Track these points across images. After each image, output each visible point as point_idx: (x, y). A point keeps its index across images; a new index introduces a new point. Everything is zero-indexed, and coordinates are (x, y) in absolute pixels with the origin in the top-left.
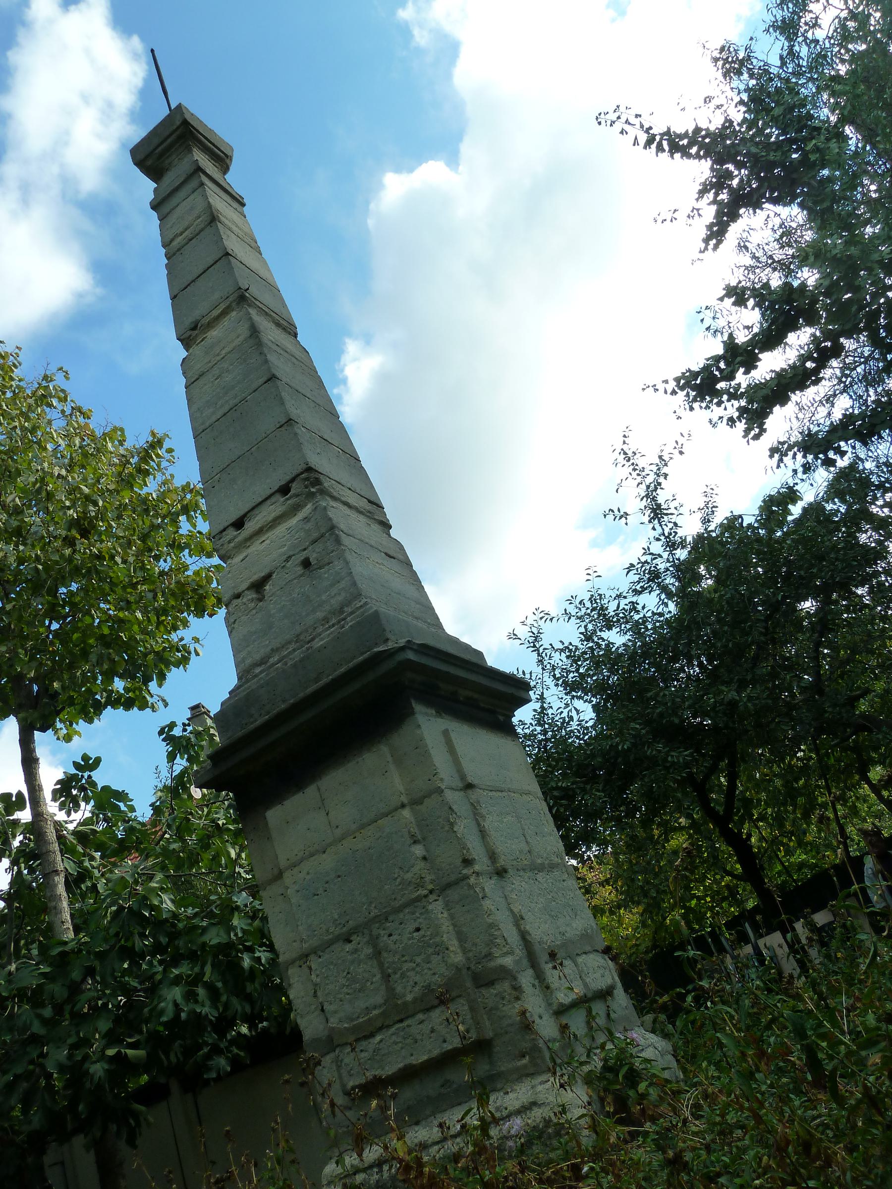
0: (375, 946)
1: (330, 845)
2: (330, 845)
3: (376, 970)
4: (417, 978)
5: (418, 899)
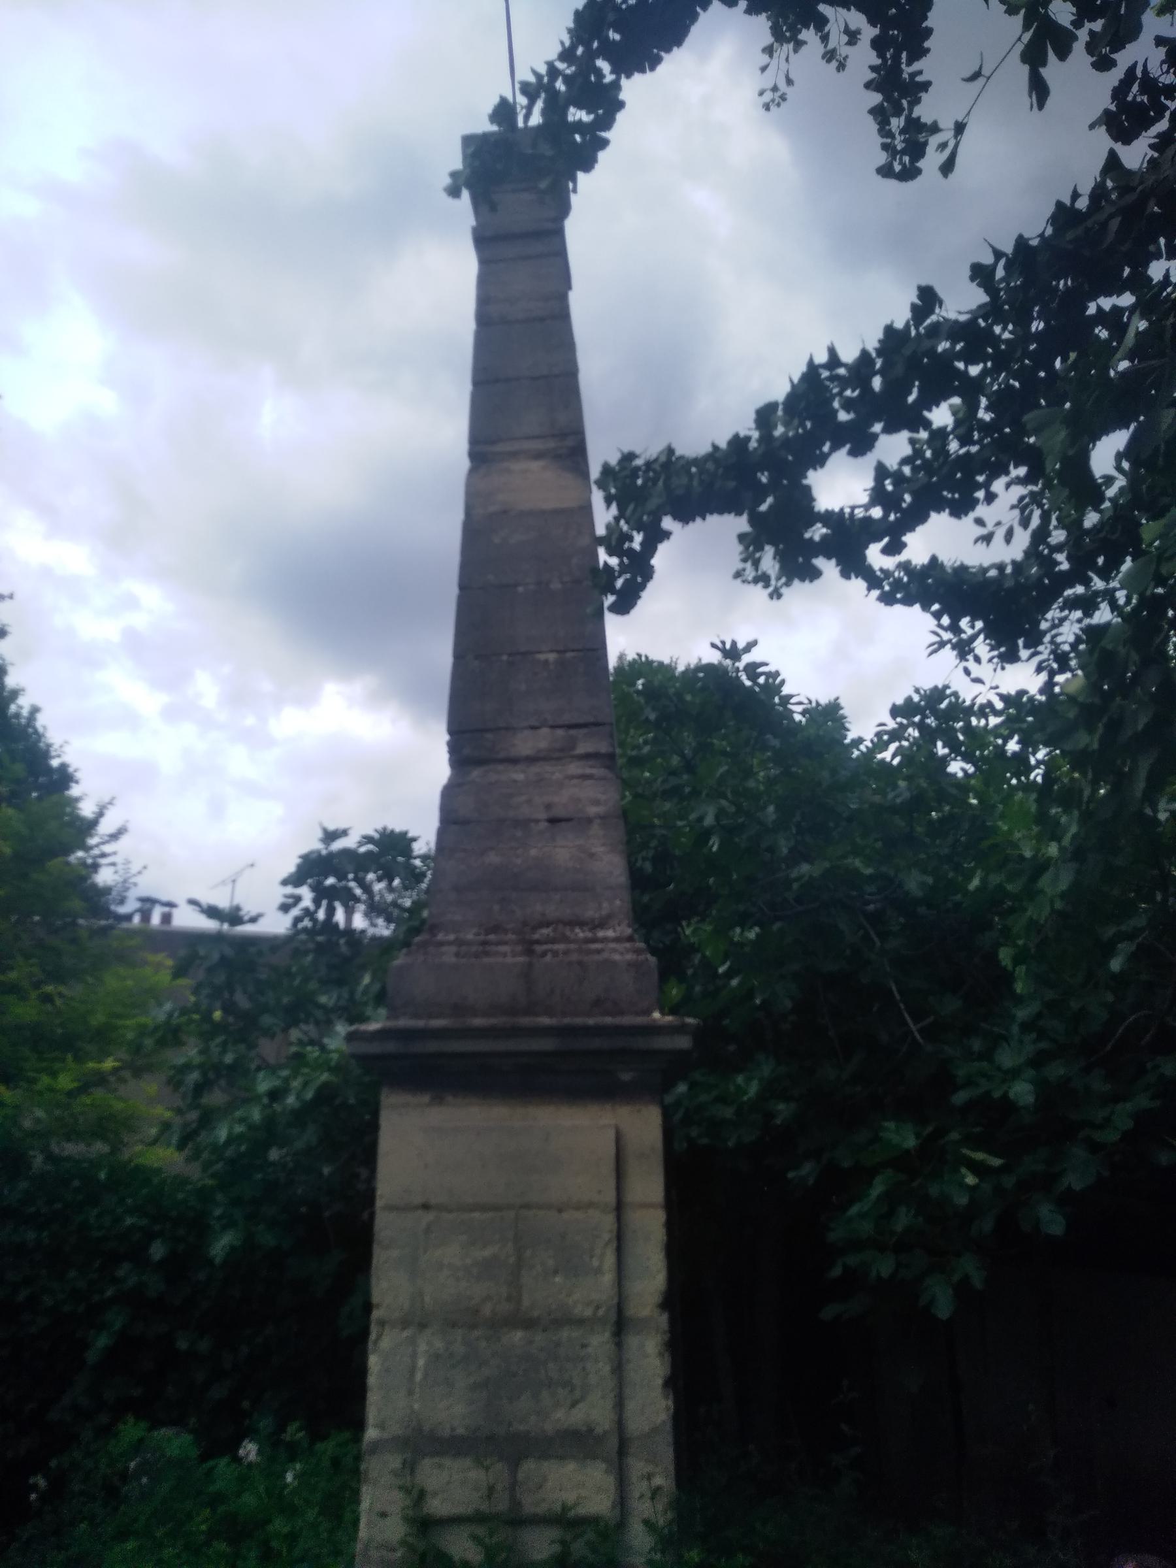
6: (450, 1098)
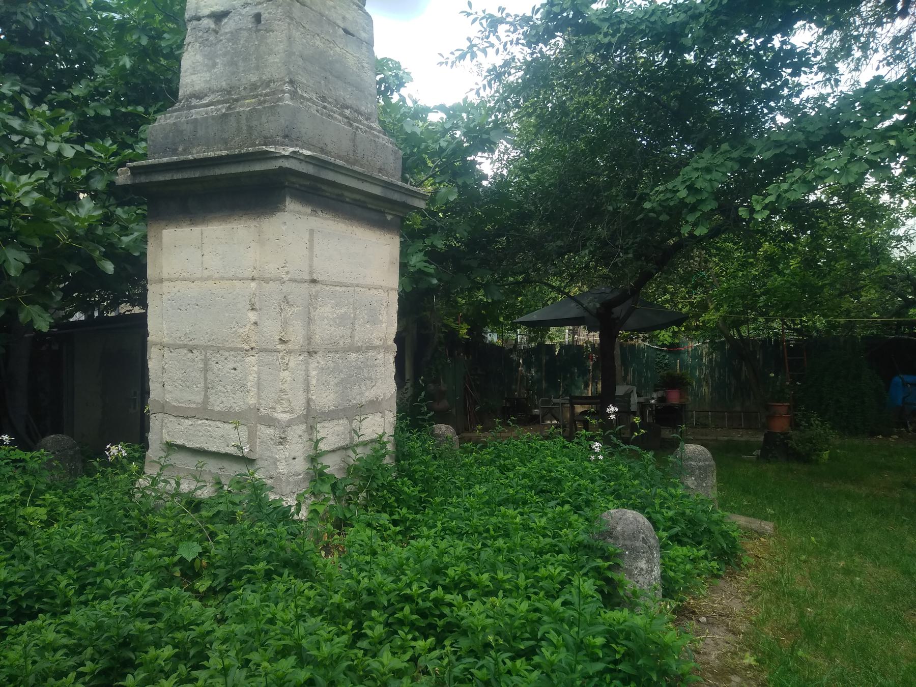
0: (206, 365)
1: (198, 279)
2: (198, 279)
3: (202, 381)
4: (224, 399)
5: (241, 350)
6: (320, 213)
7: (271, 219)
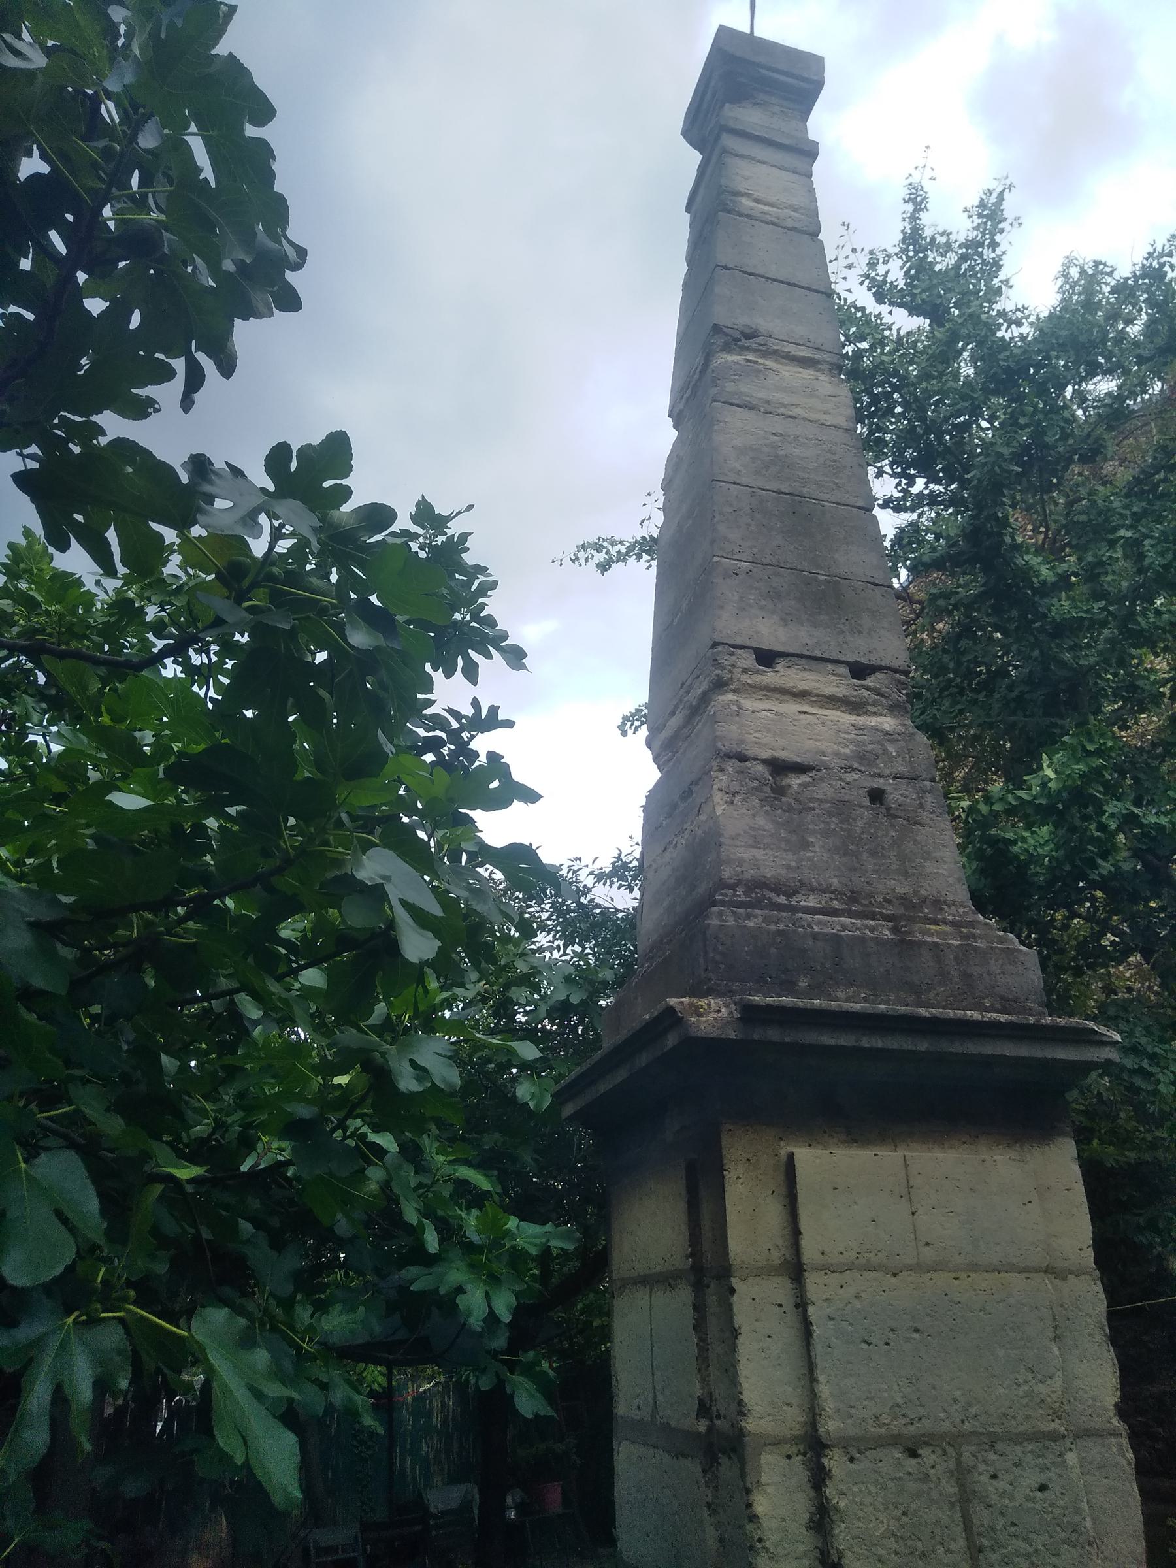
0: (961, 1485)
1: (910, 1268)
2: (910, 1268)
3: (959, 1529)
5: (1055, 1437)
7: (1036, 1151)
